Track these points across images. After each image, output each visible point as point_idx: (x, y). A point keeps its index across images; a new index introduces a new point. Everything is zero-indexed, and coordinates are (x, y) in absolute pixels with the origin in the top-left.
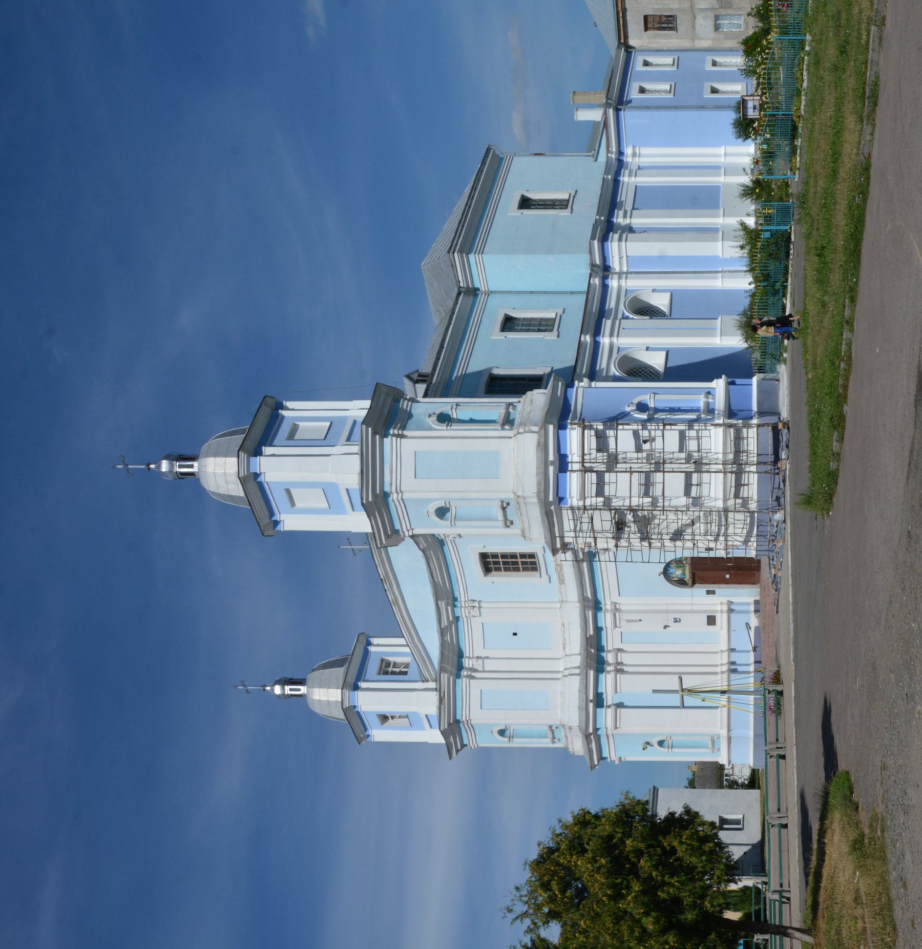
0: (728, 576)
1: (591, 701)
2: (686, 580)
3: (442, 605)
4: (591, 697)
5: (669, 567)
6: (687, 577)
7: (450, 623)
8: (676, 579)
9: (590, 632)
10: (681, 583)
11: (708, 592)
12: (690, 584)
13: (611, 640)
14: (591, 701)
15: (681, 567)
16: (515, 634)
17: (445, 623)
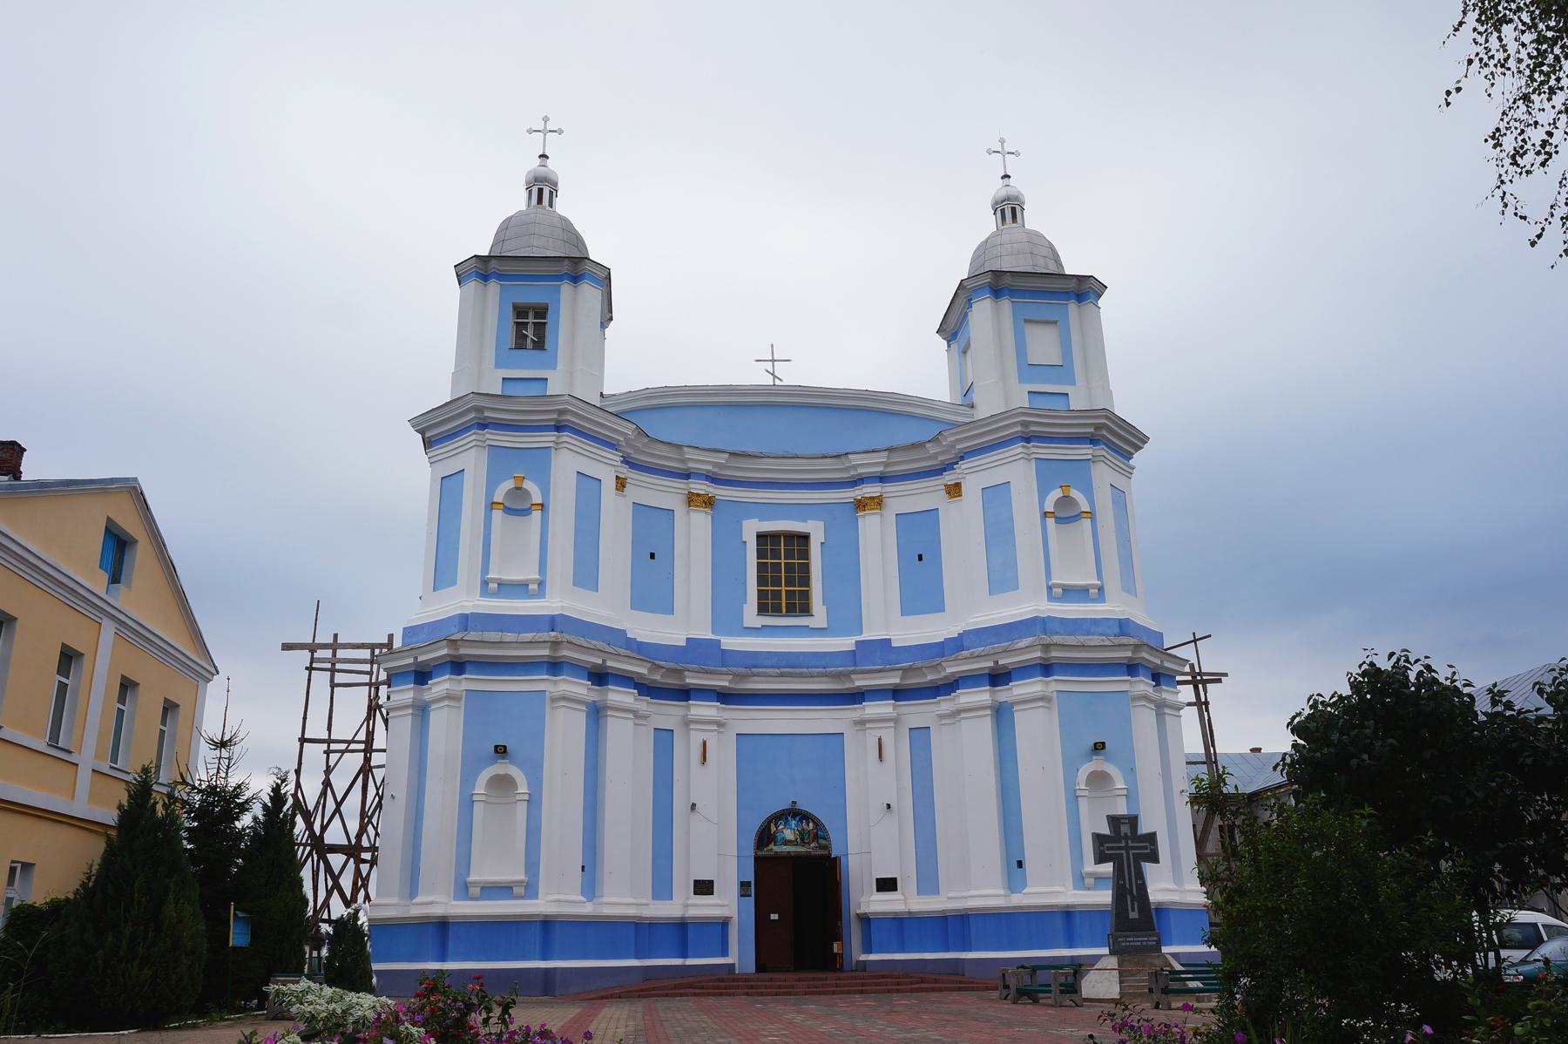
0: (774, 917)
1: (604, 661)
2: (772, 846)
3: (721, 459)
4: (609, 663)
5: (801, 821)
6: (775, 848)
7: (684, 461)
8: (773, 829)
9: (689, 677)
10: (765, 837)
11: (744, 885)
12: (760, 853)
13: (667, 714)
14: (604, 661)
15: (802, 839)
16: (652, 556)
17: (689, 454)
